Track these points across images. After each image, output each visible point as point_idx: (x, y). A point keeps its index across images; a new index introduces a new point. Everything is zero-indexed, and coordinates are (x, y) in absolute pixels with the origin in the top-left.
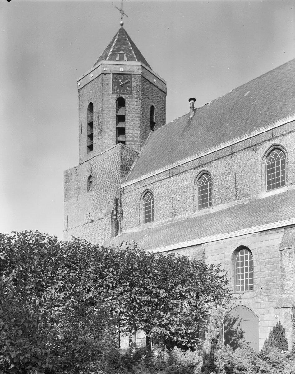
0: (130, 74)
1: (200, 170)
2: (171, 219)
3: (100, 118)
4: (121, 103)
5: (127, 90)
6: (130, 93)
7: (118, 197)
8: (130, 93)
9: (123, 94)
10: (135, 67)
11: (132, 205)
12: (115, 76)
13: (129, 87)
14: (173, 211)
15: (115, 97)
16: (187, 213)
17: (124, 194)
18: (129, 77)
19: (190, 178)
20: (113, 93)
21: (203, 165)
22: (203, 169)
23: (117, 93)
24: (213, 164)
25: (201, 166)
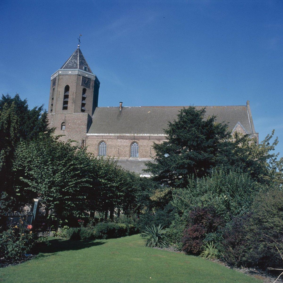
0: (90, 79)
1: (134, 141)
2: (117, 158)
3: (74, 95)
4: (84, 91)
5: (88, 86)
6: (89, 87)
7: (84, 139)
8: (89, 87)
9: (86, 87)
10: (93, 76)
11: (93, 146)
12: (83, 78)
13: (89, 84)
14: (119, 154)
15: (82, 87)
16: (126, 157)
17: (88, 139)
18: (90, 80)
19: (128, 143)
20: (82, 85)
21: (135, 139)
22: (135, 140)
23: (83, 86)
24: (140, 140)
25: (135, 139)
